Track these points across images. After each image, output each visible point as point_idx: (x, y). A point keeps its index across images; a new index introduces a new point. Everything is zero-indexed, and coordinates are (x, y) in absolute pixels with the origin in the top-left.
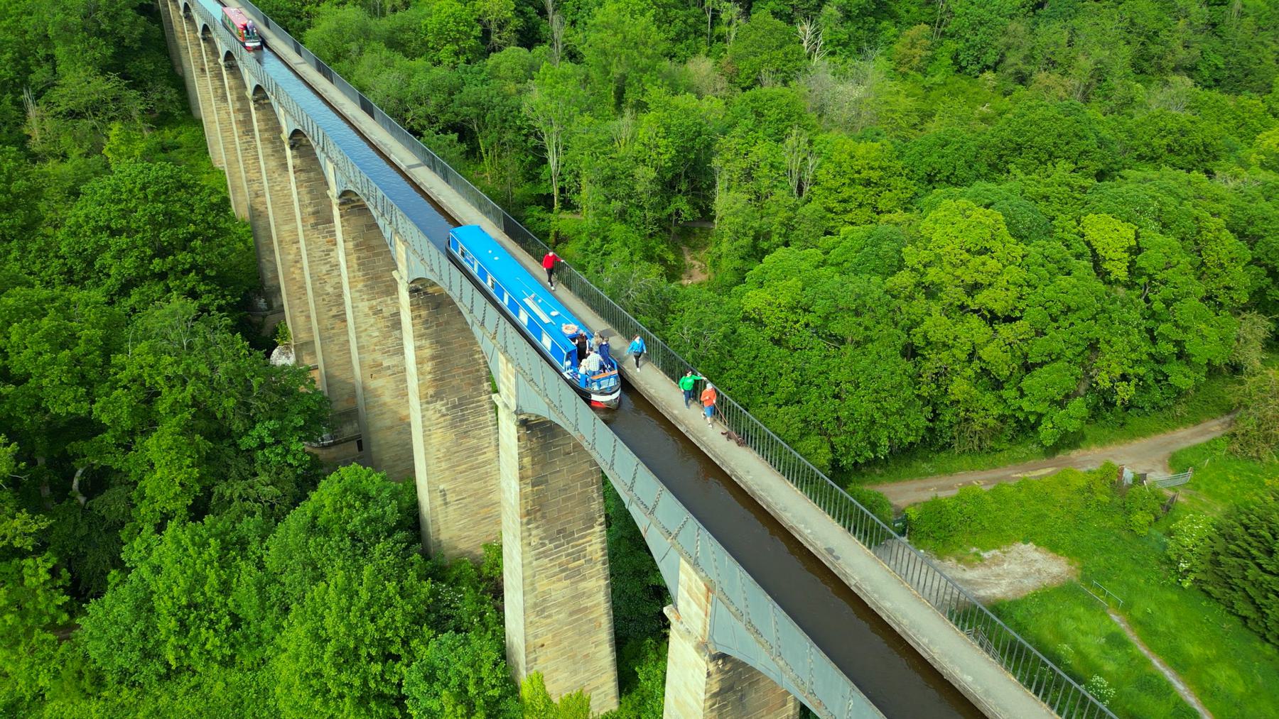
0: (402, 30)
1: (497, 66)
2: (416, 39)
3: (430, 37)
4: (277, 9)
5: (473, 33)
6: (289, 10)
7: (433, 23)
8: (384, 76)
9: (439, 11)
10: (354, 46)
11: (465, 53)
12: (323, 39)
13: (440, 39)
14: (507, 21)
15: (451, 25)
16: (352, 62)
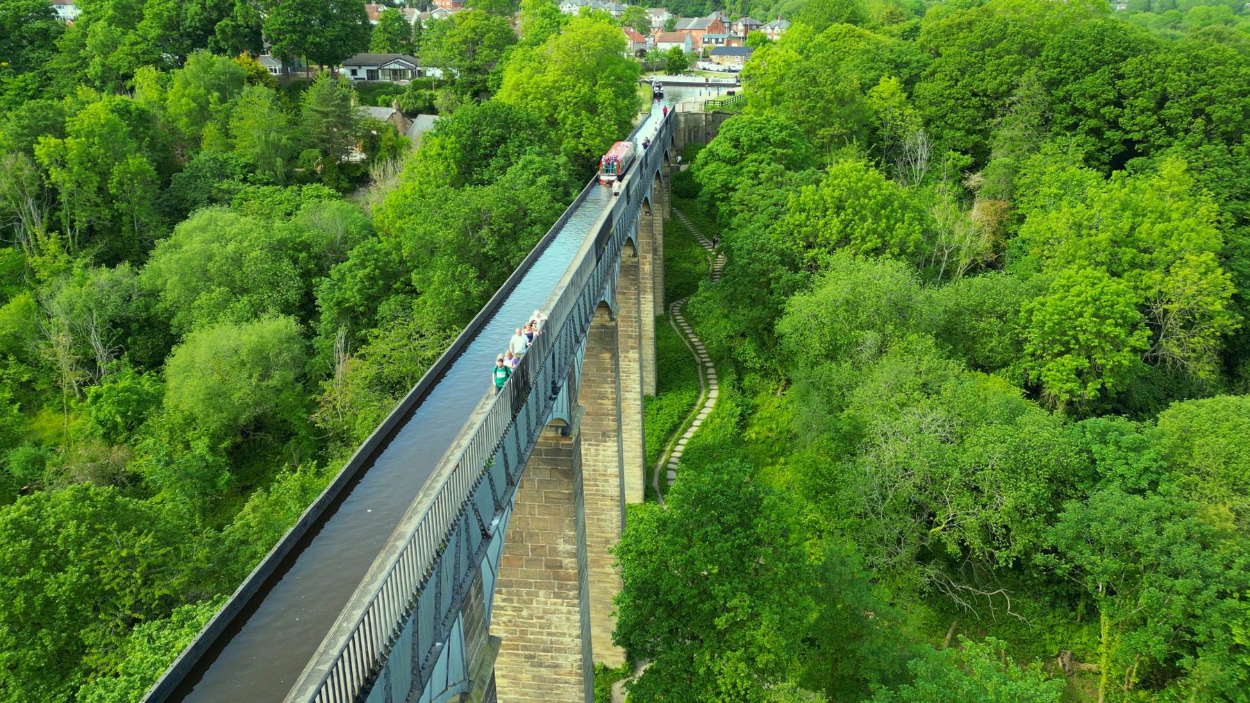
0: (977, 313)
1: (1186, 437)
2: (1001, 333)
3: (1034, 334)
4: (761, 250)
5: (1132, 341)
6: (782, 253)
7: (1047, 308)
8: (909, 420)
9: (1067, 288)
10: (871, 337)
11: (1099, 375)
12: (816, 316)
13: (1054, 342)
14: (1208, 317)
15: (1086, 320)
16: (856, 366)
